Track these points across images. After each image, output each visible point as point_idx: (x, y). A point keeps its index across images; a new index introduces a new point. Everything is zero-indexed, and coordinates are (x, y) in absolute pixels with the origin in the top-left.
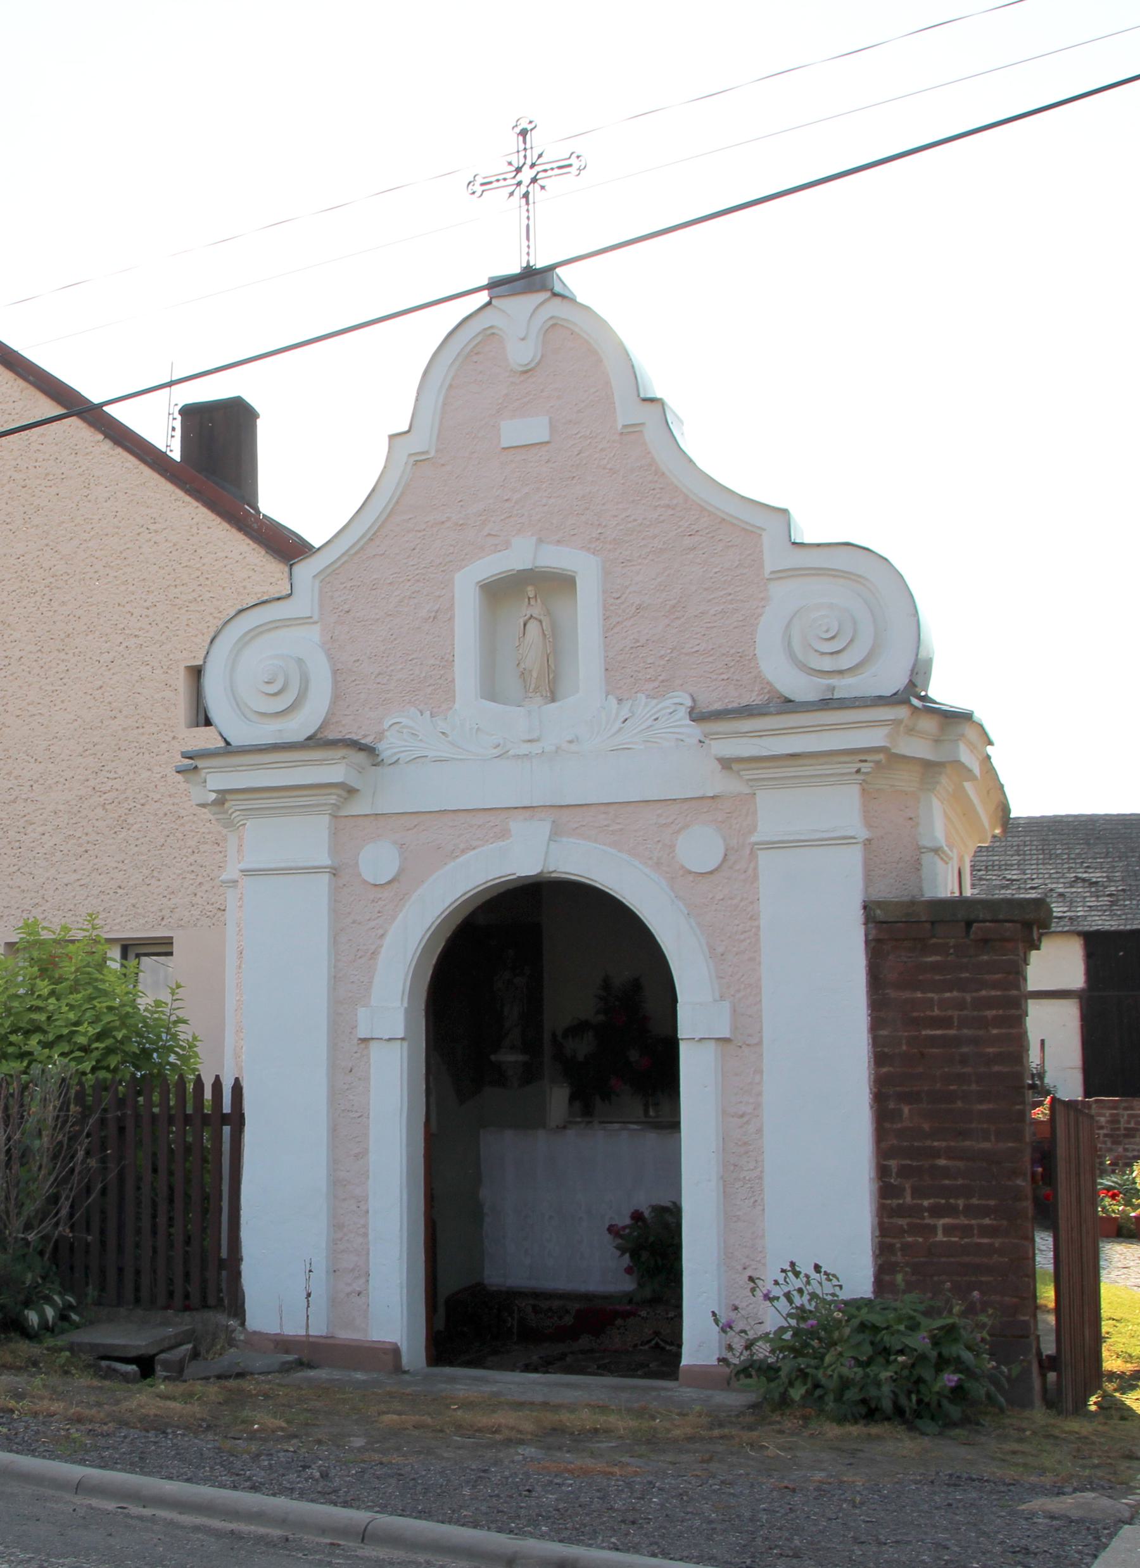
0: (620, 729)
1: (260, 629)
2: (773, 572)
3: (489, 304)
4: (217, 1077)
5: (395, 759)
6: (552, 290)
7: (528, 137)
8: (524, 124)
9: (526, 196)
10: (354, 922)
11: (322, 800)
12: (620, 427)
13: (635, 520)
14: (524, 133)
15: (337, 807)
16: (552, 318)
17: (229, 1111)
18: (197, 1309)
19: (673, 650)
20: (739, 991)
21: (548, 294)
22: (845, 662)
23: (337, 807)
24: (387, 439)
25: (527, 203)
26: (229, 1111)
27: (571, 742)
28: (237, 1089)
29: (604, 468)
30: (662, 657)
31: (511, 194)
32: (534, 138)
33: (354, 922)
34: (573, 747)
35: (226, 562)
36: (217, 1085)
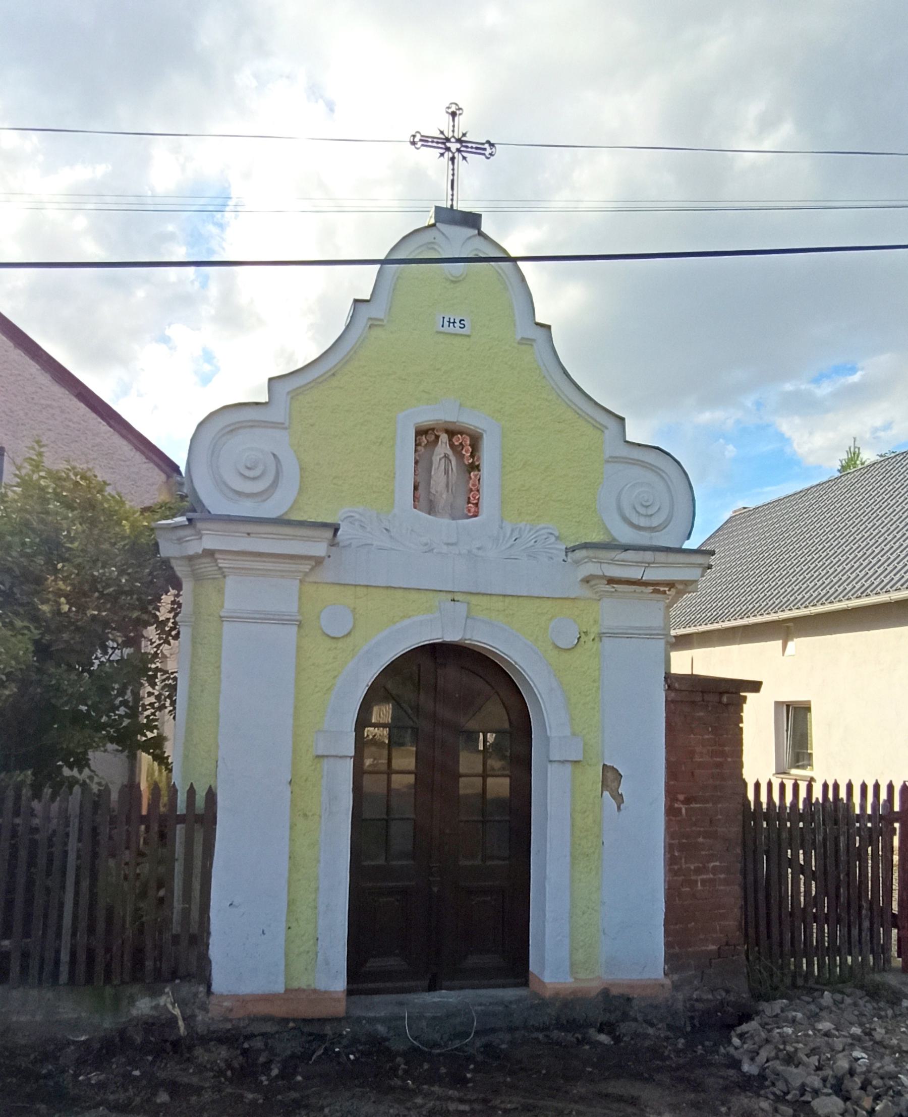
0: (512, 545)
1: (244, 424)
2: (611, 457)
3: (434, 225)
4: (891, 782)
5: (348, 542)
6: (479, 229)
7: (456, 119)
8: (453, 108)
9: (453, 159)
10: (313, 664)
11: (293, 567)
12: (519, 338)
13: (525, 404)
14: (454, 114)
15: (306, 574)
16: (476, 249)
17: (184, 812)
18: (128, 983)
19: (546, 496)
20: (584, 729)
21: (476, 232)
22: (655, 522)
23: (306, 574)
24: (351, 301)
25: (453, 164)
26: (184, 812)
27: (479, 549)
28: (211, 796)
29: (506, 363)
30: (538, 500)
31: (442, 155)
32: (461, 120)
33: (313, 664)
34: (480, 553)
35: (20, 378)
36: (191, 792)
